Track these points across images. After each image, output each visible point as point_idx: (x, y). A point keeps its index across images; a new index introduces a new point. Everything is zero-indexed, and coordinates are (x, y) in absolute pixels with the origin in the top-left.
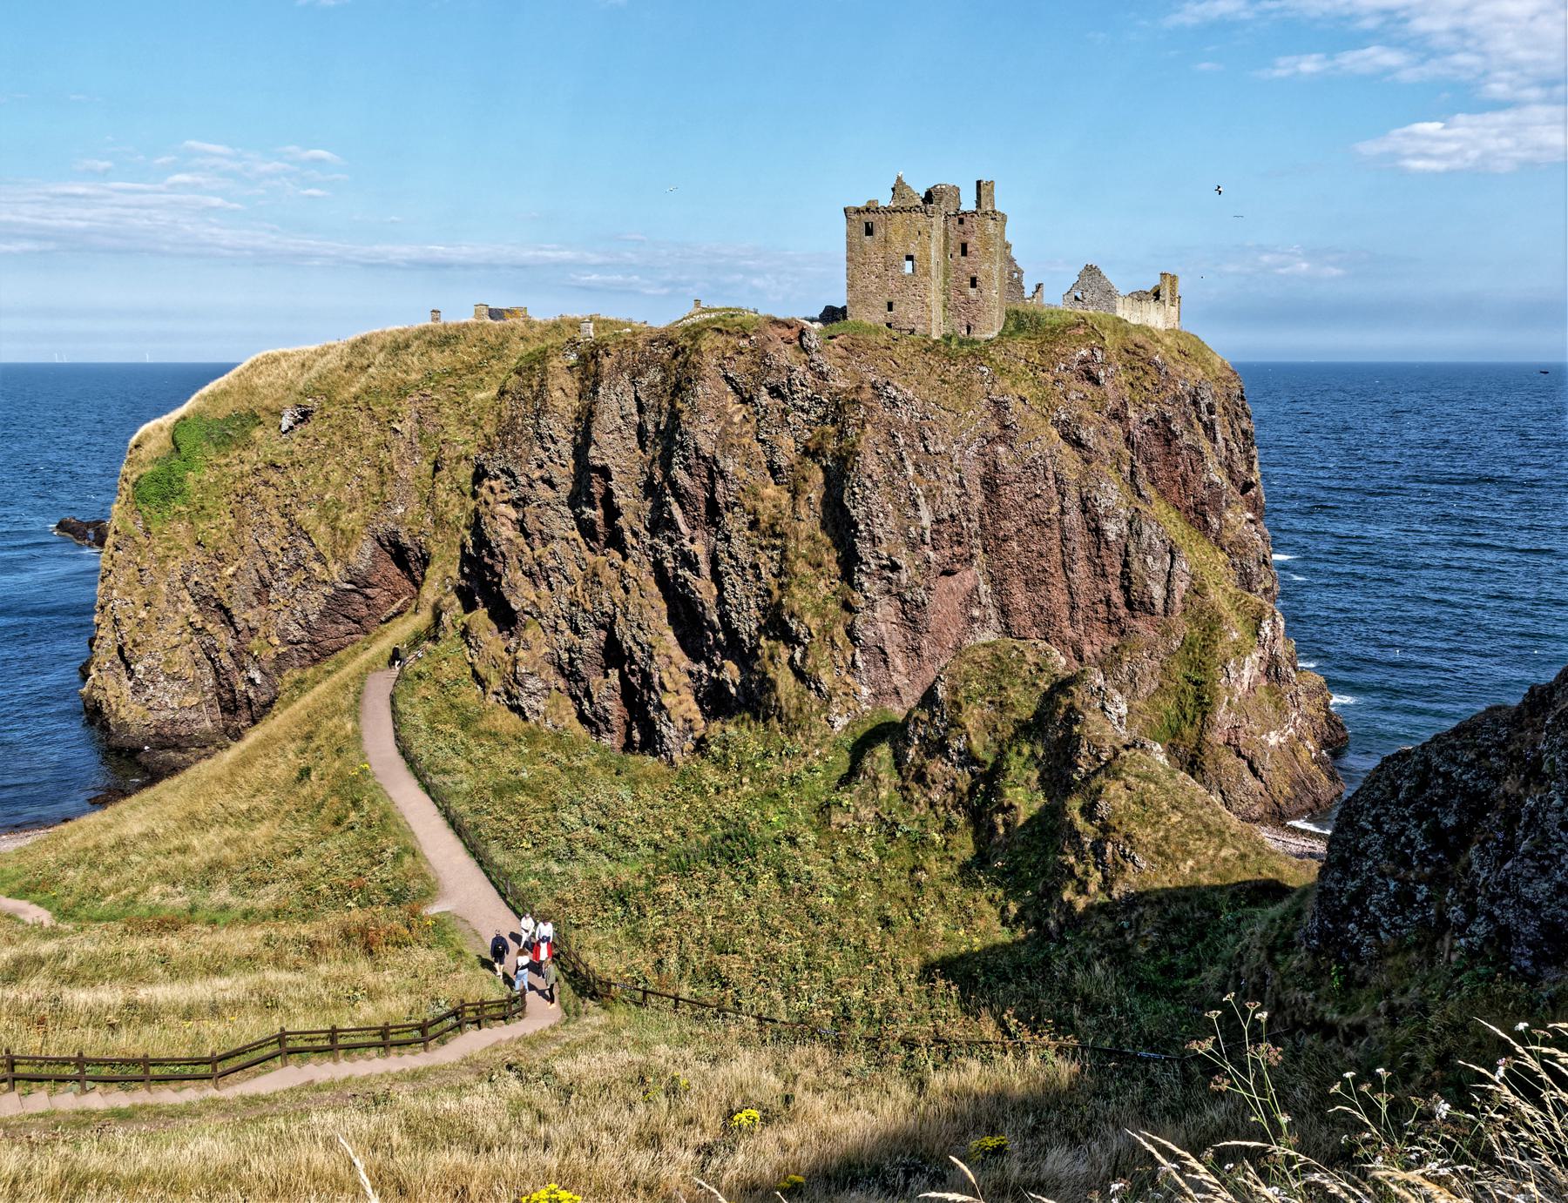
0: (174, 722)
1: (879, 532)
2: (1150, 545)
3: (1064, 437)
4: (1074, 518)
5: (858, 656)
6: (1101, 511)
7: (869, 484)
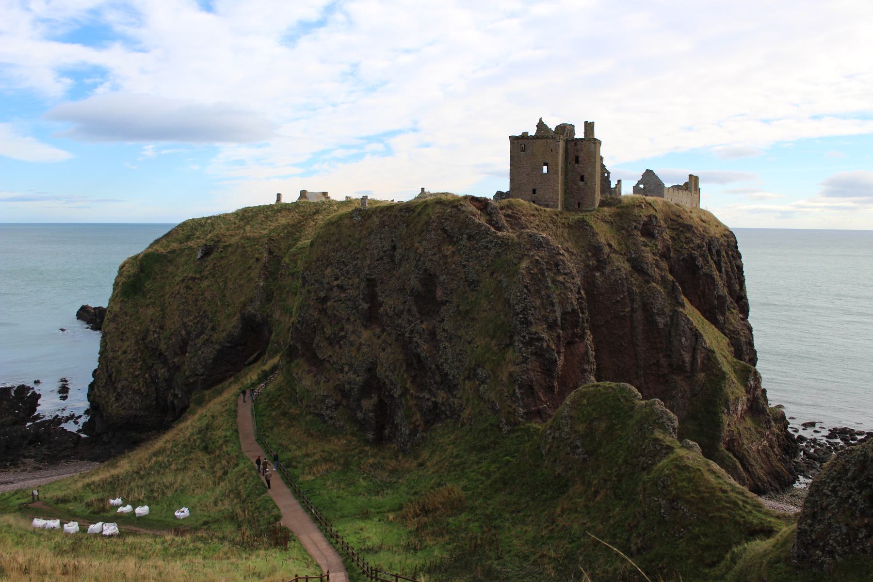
0: (136, 416)
1: (531, 318)
2: (683, 331)
4: (639, 316)
5: (517, 391)
6: (655, 311)
7: (525, 290)
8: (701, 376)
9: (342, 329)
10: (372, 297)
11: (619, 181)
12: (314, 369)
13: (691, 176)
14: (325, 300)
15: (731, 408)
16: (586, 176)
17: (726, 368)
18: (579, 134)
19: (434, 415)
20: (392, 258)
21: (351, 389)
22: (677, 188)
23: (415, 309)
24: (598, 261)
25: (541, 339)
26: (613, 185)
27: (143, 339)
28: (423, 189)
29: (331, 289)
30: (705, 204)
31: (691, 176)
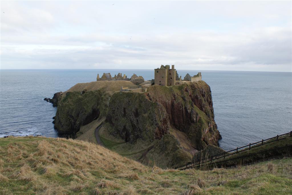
3: (183, 99)
4: (184, 110)
6: (188, 109)
9: (118, 117)
10: (125, 111)
11: (181, 76)
12: (112, 125)
13: (199, 73)
14: (114, 110)
15: (204, 131)
16: (172, 77)
17: (204, 121)
18: (171, 68)
19: (137, 137)
20: (129, 104)
21: (120, 130)
22: (195, 76)
23: (134, 115)
24: (175, 98)
25: (158, 124)
26: (179, 78)
27: (68, 113)
28: (134, 74)
29: (116, 108)
31: (199, 73)
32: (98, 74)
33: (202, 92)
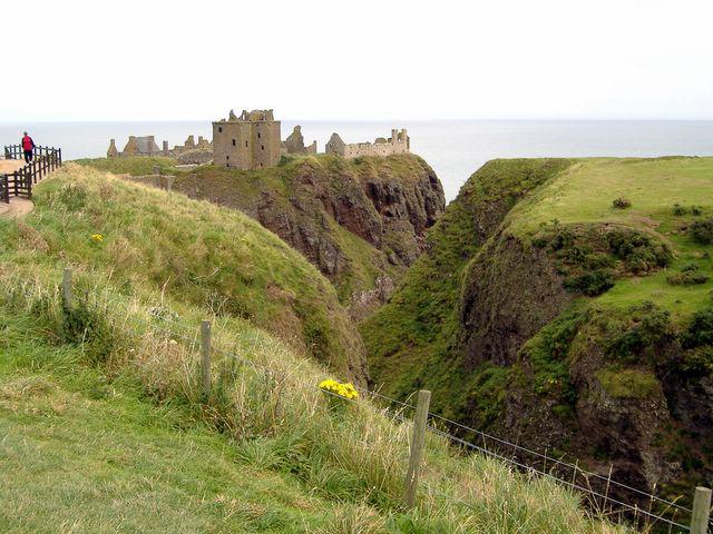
8: (339, 276)
26: (307, 143)
30: (414, 150)
32: (113, 141)
33: (386, 187)
